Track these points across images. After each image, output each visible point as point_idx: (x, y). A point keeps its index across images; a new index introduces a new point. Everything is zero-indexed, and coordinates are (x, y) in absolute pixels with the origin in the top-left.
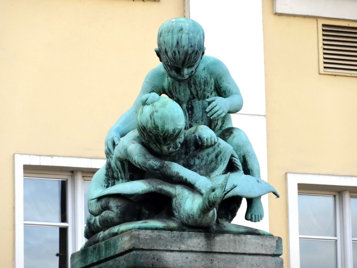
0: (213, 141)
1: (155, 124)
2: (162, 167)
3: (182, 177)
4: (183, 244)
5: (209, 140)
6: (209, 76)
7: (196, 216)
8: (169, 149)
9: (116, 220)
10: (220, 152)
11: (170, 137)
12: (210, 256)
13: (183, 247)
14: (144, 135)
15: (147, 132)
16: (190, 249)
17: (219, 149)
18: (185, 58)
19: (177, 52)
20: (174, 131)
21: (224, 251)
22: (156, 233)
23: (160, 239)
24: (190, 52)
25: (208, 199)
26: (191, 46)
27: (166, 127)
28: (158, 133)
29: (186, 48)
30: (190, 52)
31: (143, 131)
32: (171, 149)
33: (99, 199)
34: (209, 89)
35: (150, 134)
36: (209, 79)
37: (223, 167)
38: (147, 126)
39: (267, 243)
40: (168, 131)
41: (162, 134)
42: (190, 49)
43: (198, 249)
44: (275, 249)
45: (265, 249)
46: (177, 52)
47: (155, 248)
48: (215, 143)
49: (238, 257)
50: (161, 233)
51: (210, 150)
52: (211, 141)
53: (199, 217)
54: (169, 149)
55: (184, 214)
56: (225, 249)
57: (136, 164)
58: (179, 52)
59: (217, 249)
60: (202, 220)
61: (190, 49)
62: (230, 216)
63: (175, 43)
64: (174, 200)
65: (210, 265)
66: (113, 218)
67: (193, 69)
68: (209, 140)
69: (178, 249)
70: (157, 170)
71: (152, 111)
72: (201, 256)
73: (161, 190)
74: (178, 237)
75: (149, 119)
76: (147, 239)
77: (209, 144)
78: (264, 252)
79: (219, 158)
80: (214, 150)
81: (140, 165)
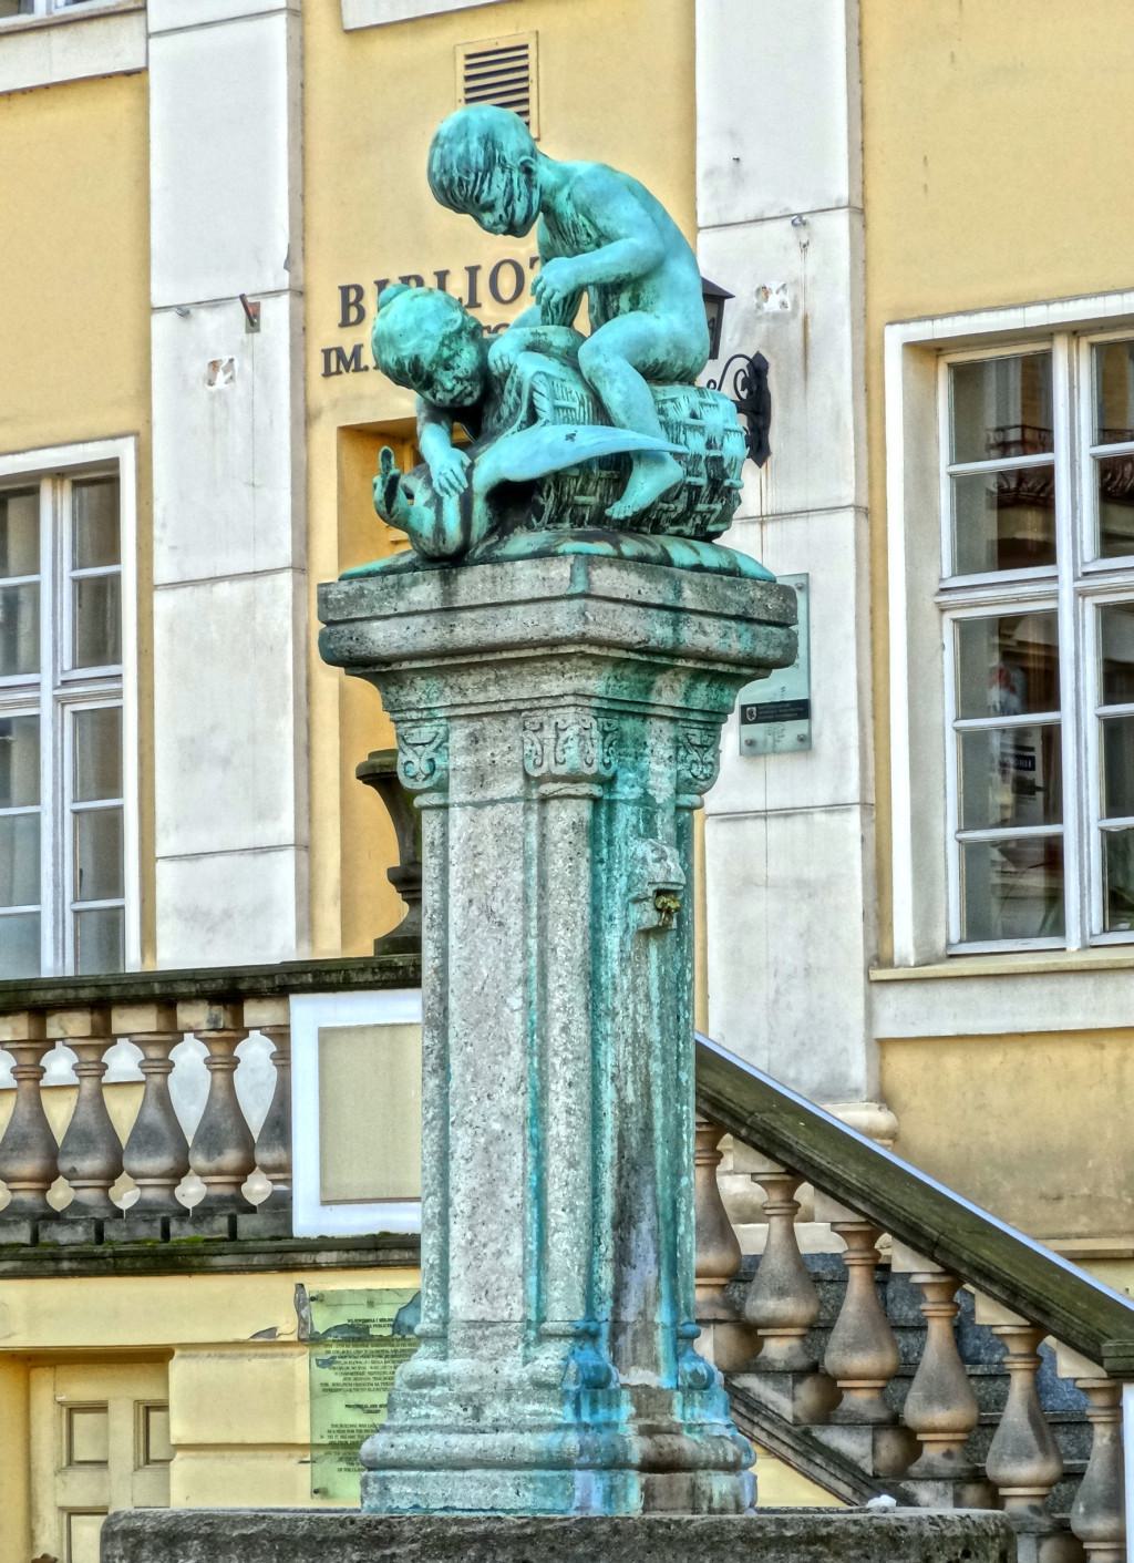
0: (506, 362)
4: (402, 599)
5: (499, 363)
8: (434, 396)
12: (447, 618)
13: (402, 607)
16: (413, 608)
20: (399, 362)
22: (356, 584)
23: (363, 596)
26: (445, 172)
30: (445, 183)
32: (439, 396)
34: (584, 237)
37: (523, 415)
39: (553, 574)
44: (566, 583)
45: (550, 587)
47: (353, 616)
49: (500, 612)
50: (364, 585)
56: (476, 598)
59: (461, 601)
62: (534, 520)
65: (447, 636)
67: (500, 211)
68: (499, 363)
69: (392, 612)
72: (433, 619)
74: (393, 587)
77: (501, 370)
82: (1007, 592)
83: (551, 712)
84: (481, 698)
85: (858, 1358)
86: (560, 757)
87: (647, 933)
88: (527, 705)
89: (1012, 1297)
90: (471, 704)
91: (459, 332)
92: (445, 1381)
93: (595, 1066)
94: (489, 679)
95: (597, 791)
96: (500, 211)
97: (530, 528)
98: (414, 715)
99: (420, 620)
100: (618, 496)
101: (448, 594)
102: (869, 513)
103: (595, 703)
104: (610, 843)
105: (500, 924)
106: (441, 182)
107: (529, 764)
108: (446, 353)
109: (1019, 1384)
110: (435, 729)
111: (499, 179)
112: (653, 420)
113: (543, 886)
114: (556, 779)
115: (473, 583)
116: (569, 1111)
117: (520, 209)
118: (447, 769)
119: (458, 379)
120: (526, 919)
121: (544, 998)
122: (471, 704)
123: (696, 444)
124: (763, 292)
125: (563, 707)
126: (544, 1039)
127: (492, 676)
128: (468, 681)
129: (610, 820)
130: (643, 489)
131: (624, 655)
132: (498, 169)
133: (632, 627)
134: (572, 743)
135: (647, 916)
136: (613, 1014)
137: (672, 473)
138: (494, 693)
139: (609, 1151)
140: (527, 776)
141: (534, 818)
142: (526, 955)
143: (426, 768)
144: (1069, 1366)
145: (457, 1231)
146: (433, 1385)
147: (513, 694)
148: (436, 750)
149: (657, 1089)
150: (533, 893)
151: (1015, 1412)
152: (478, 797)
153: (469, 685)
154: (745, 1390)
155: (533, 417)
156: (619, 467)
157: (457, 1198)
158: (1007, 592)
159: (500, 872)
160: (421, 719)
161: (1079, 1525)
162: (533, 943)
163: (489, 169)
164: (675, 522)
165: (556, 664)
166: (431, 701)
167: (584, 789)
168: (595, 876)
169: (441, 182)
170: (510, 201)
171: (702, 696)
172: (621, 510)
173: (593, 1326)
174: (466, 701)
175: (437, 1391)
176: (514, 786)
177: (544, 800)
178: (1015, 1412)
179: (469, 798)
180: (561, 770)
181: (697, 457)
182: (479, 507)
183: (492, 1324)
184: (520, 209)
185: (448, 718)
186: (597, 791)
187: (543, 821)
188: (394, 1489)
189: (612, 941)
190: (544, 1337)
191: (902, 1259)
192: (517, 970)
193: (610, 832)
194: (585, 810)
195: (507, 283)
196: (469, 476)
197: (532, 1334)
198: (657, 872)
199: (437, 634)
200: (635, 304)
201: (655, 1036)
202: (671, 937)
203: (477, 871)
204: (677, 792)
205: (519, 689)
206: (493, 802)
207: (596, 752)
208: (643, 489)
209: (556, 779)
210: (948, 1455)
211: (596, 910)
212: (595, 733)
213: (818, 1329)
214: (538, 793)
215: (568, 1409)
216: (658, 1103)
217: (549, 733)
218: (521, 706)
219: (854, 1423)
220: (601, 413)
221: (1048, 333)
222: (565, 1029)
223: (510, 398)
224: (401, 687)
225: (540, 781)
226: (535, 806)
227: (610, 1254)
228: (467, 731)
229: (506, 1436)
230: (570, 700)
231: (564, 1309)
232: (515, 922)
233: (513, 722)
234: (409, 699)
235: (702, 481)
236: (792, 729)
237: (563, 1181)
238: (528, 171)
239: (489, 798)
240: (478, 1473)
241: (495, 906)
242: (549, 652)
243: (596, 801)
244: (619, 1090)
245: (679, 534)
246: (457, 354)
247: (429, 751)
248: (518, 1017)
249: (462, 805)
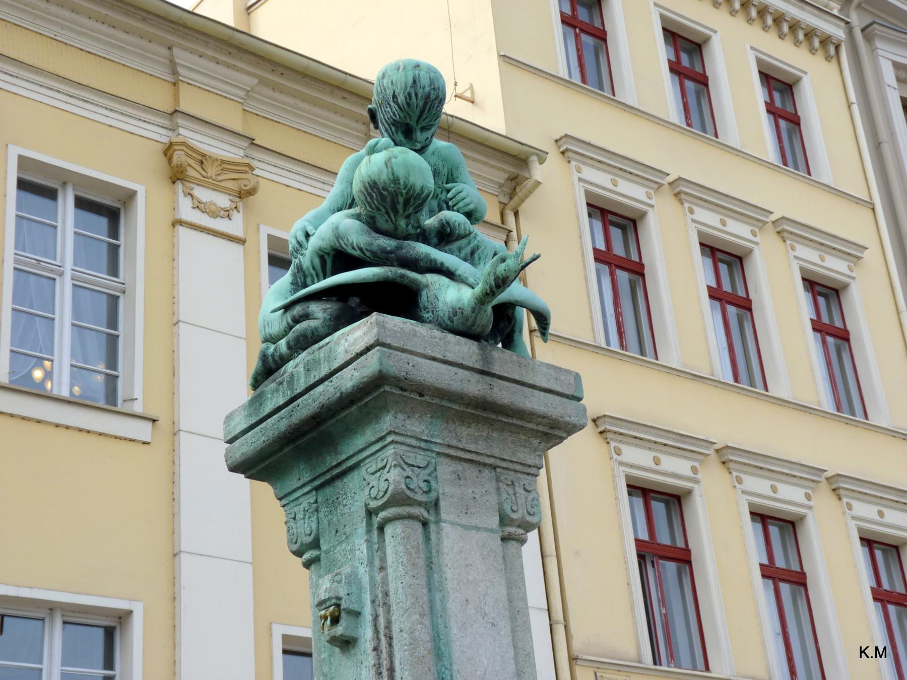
1: (393, 174)
2: (399, 248)
3: (435, 261)
6: (441, 163)
7: (468, 311)
9: (322, 331)
10: (478, 247)
11: (415, 198)
14: (371, 197)
15: (378, 189)
17: (476, 242)
18: (425, 104)
19: (413, 95)
20: (422, 189)
21: (506, 375)
23: (415, 335)
24: (433, 96)
25: (494, 274)
27: (412, 180)
28: (399, 188)
29: (427, 89)
31: (372, 189)
33: (287, 308)
35: (385, 193)
36: (441, 168)
38: (379, 179)
40: (412, 187)
41: (404, 191)
42: (432, 92)
43: (470, 364)
46: (413, 95)
48: (470, 233)
51: (463, 242)
52: (465, 230)
53: (473, 312)
54: (407, 226)
55: (445, 308)
57: (354, 249)
58: (416, 95)
59: (496, 370)
60: (476, 318)
61: (432, 92)
63: (410, 81)
64: (424, 293)
66: (316, 328)
70: (391, 252)
71: (387, 157)
72: (477, 377)
73: (403, 276)
75: (384, 167)
76: (396, 332)
77: (462, 232)
78: (559, 389)
79: (476, 256)
80: (469, 243)
81: (361, 249)
83: (519, 475)
84: (472, 447)
86: (532, 511)
88: (504, 464)
90: (462, 449)
94: (481, 436)
98: (413, 442)
105: (493, 625)
106: (429, 94)
107: (507, 508)
110: (428, 459)
118: (438, 493)
122: (462, 449)
125: (528, 474)
127: (484, 434)
128: (464, 431)
138: (481, 447)
147: (496, 452)
148: (430, 475)
152: (465, 521)
153: (465, 433)
159: (488, 584)
160: (419, 448)
165: (536, 442)
166: (432, 437)
169: (429, 94)
174: (461, 446)
179: (458, 520)
185: (438, 453)
199: (480, 386)
203: (470, 578)
206: (478, 529)
218: (499, 463)
224: (409, 417)
225: (512, 522)
228: (451, 468)
233: (487, 473)
234: (413, 428)
239: (474, 524)
241: (487, 609)
247: (424, 474)
249: (452, 523)
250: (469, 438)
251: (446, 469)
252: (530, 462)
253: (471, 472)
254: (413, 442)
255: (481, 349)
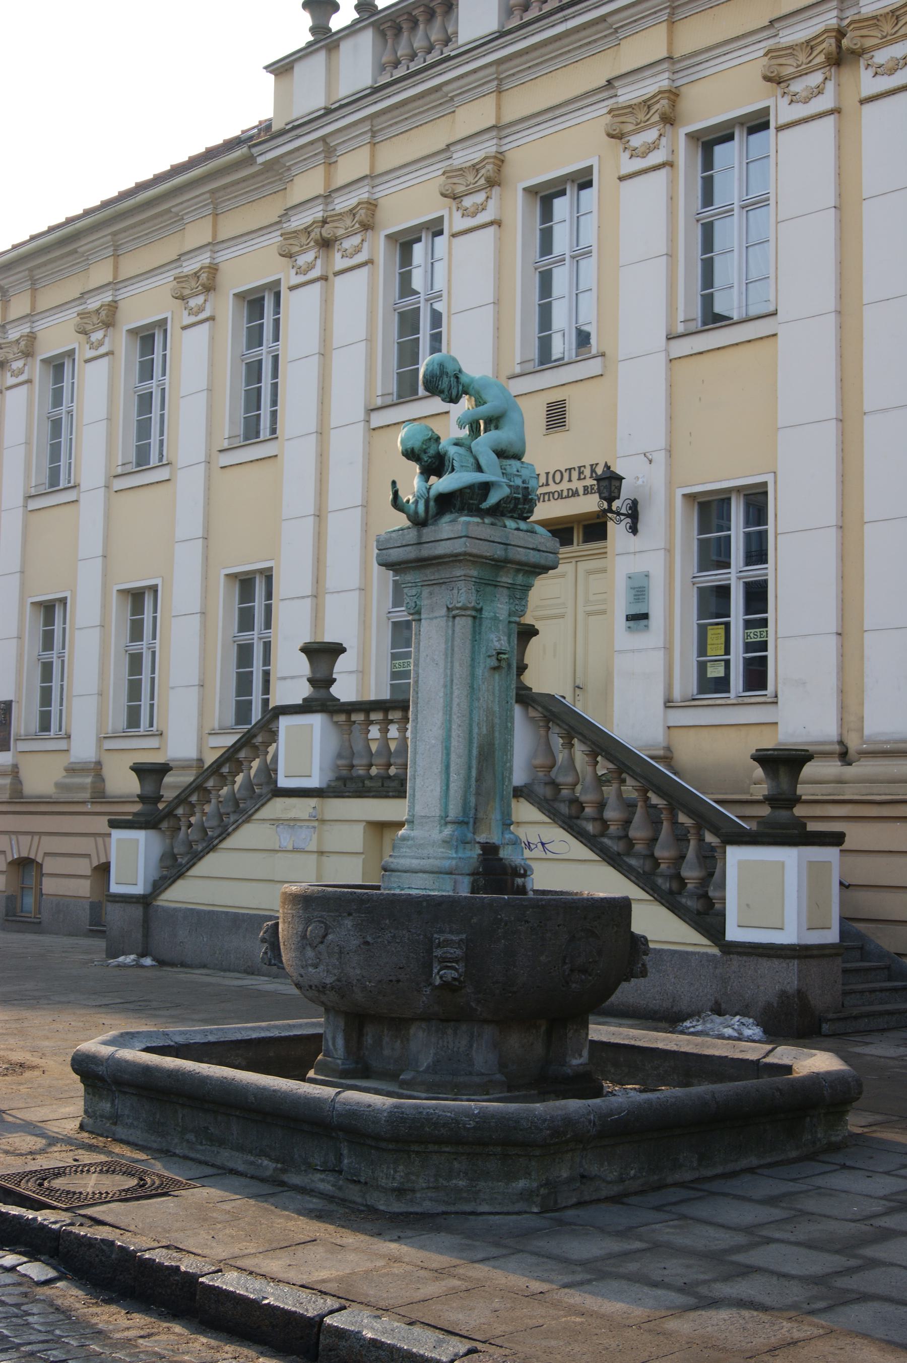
12: (419, 546)
37: (450, 469)
49: (437, 544)
59: (424, 540)
67: (446, 393)
72: (414, 547)
82: (714, 578)
84: (432, 578)
85: (638, 832)
87: (495, 669)
89: (690, 813)
91: (430, 439)
92: (413, 839)
93: (471, 719)
95: (474, 613)
96: (446, 393)
97: (451, 512)
98: (410, 585)
99: (410, 548)
100: (485, 500)
101: (420, 536)
102: (669, 551)
103: (474, 579)
104: (480, 633)
108: (424, 447)
109: (693, 843)
111: (445, 379)
112: (499, 472)
113: (453, 650)
114: (458, 608)
115: (428, 533)
116: (459, 736)
117: (454, 393)
119: (430, 457)
120: (446, 662)
121: (452, 693)
123: (518, 482)
124: (638, 478)
126: (451, 708)
128: (428, 571)
129: (480, 625)
130: (494, 498)
131: (484, 560)
132: (445, 376)
133: (486, 550)
134: (464, 595)
135: (494, 662)
136: (478, 699)
137: (506, 491)
139: (475, 752)
140: (448, 608)
141: (450, 624)
142: (446, 676)
143: (413, 605)
144: (709, 838)
145: (418, 781)
146: (408, 840)
147: (443, 576)
149: (497, 728)
150: (449, 652)
151: (691, 853)
152: (431, 616)
154: (601, 843)
155: (453, 470)
156: (486, 488)
157: (418, 769)
158: (714, 578)
161: (711, 894)
162: (449, 672)
163: (441, 376)
164: (510, 512)
167: (469, 612)
168: (473, 646)
170: (450, 389)
171: (520, 579)
172: (485, 505)
173: (466, 820)
175: (410, 843)
176: (444, 611)
177: (454, 617)
178: (691, 853)
180: (459, 605)
181: (518, 487)
182: (432, 503)
183: (429, 817)
184: (454, 393)
186: (474, 613)
187: (454, 625)
188: (392, 879)
189: (479, 672)
190: (446, 823)
191: (655, 799)
192: (442, 683)
193: (480, 630)
194: (470, 621)
195: (558, 479)
196: (428, 493)
197: (443, 822)
198: (497, 645)
200: (497, 428)
201: (496, 709)
202: (504, 671)
204: (509, 615)
205: (445, 573)
206: (436, 618)
207: (473, 598)
208: (494, 498)
209: (458, 608)
210: (668, 867)
211: (473, 659)
212: (474, 591)
213: (627, 823)
214: (452, 614)
215: (454, 851)
216: (497, 734)
217: (455, 591)
219: (637, 856)
220: (479, 469)
221: (729, 490)
222: (458, 704)
223: (447, 464)
226: (451, 619)
227: (474, 792)
229: (431, 860)
230: (463, 578)
231: (454, 812)
232: (442, 664)
233: (444, 586)
235: (520, 496)
236: (644, 622)
237: (457, 762)
238: (457, 378)
240: (420, 875)
241: (435, 657)
242: (455, 559)
243: (474, 617)
244: (479, 728)
245: (512, 517)
246: (429, 447)
248: (442, 700)
249: (426, 619)
250: (431, 574)
251: (426, 592)
252: (458, 575)
253: (436, 588)
254: (410, 585)
255: (418, 531)
